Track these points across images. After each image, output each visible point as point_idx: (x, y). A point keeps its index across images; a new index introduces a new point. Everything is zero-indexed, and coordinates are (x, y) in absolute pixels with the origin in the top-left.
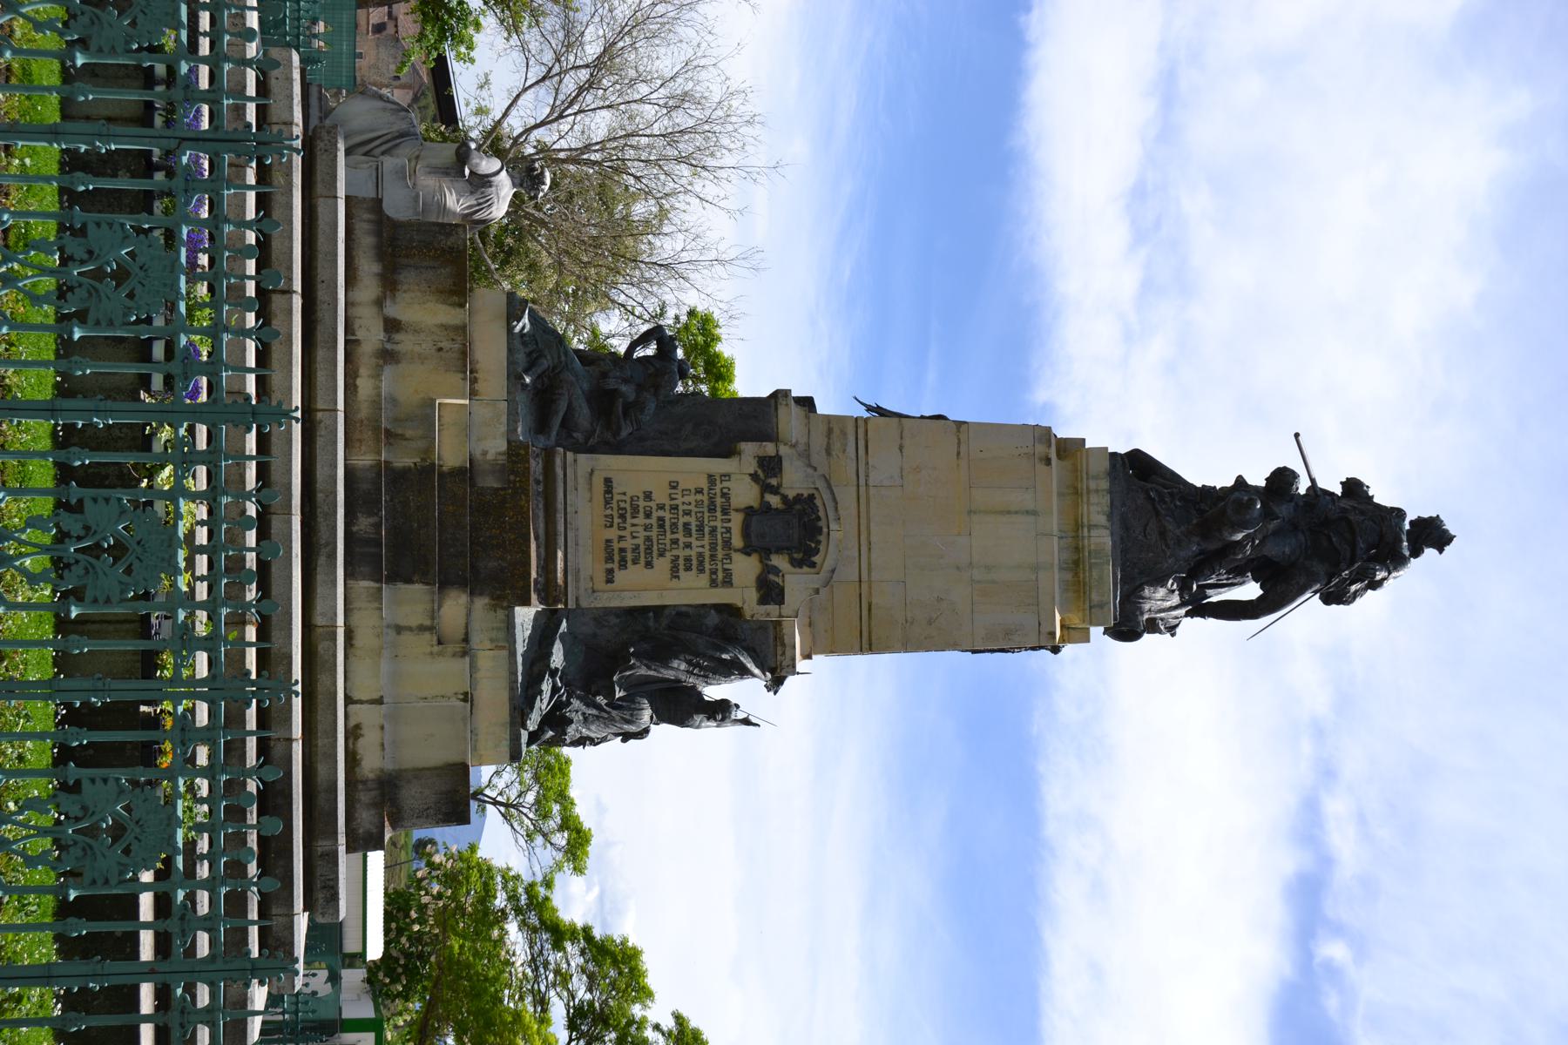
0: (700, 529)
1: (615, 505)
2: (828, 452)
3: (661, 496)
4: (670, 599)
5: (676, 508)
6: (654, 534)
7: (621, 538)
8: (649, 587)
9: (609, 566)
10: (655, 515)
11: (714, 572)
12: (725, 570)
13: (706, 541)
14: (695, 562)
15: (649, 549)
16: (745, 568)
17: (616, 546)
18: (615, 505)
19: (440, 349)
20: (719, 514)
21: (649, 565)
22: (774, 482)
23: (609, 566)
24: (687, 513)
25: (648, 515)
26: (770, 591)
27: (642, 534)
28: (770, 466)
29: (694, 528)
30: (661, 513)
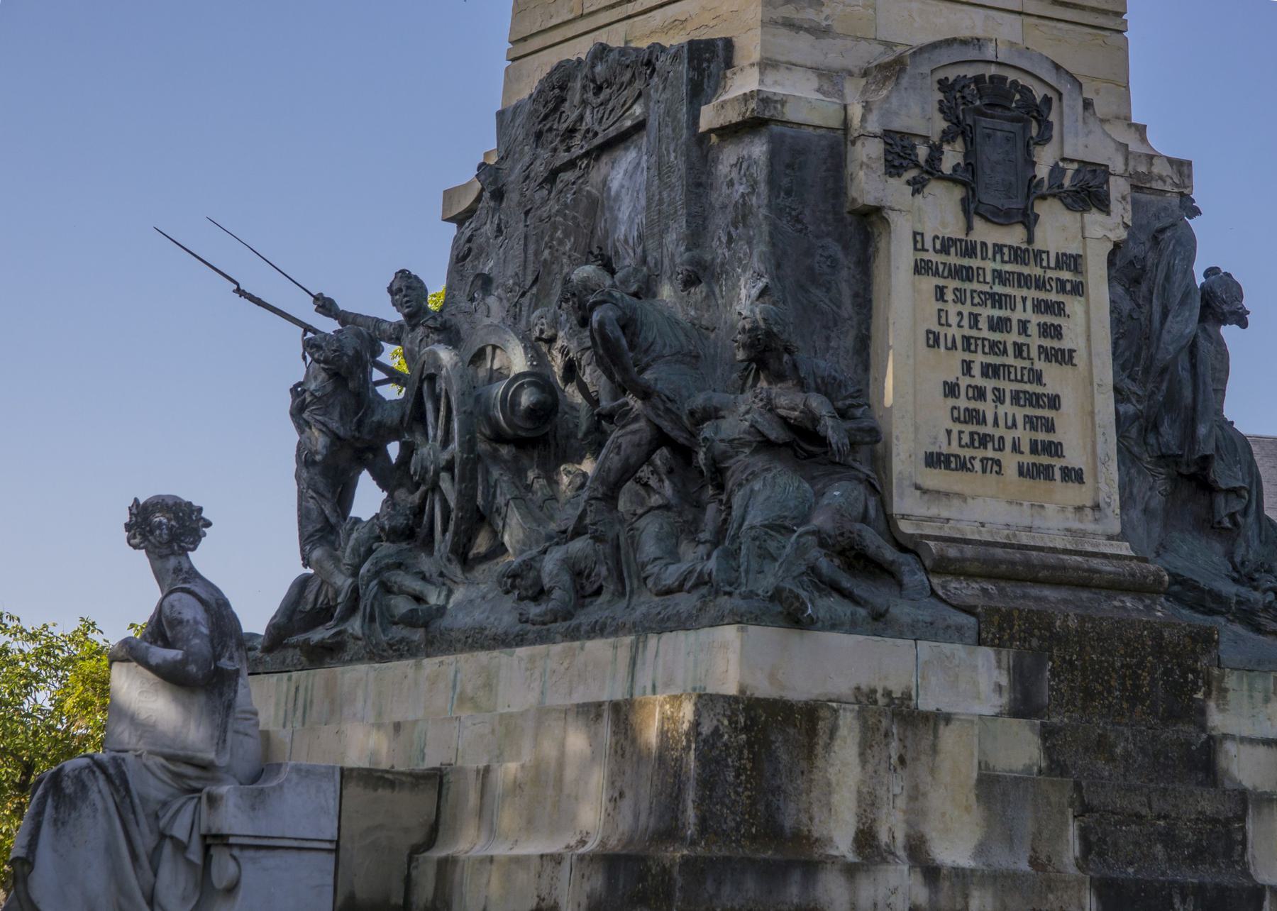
2: (819, 32)
3: (949, 366)
4: (1105, 372)
5: (966, 339)
6: (1008, 387)
7: (1016, 448)
10: (979, 381)
11: (1062, 285)
12: (1058, 266)
13: (1017, 292)
15: (1034, 400)
16: (1057, 229)
17: (1028, 459)
18: (967, 453)
19: (902, 760)
20: (975, 263)
21: (1054, 402)
22: (922, 152)
24: (975, 318)
25: (980, 394)
26: (1088, 192)
27: (1007, 408)
28: (899, 153)
29: (997, 313)
30: (976, 370)
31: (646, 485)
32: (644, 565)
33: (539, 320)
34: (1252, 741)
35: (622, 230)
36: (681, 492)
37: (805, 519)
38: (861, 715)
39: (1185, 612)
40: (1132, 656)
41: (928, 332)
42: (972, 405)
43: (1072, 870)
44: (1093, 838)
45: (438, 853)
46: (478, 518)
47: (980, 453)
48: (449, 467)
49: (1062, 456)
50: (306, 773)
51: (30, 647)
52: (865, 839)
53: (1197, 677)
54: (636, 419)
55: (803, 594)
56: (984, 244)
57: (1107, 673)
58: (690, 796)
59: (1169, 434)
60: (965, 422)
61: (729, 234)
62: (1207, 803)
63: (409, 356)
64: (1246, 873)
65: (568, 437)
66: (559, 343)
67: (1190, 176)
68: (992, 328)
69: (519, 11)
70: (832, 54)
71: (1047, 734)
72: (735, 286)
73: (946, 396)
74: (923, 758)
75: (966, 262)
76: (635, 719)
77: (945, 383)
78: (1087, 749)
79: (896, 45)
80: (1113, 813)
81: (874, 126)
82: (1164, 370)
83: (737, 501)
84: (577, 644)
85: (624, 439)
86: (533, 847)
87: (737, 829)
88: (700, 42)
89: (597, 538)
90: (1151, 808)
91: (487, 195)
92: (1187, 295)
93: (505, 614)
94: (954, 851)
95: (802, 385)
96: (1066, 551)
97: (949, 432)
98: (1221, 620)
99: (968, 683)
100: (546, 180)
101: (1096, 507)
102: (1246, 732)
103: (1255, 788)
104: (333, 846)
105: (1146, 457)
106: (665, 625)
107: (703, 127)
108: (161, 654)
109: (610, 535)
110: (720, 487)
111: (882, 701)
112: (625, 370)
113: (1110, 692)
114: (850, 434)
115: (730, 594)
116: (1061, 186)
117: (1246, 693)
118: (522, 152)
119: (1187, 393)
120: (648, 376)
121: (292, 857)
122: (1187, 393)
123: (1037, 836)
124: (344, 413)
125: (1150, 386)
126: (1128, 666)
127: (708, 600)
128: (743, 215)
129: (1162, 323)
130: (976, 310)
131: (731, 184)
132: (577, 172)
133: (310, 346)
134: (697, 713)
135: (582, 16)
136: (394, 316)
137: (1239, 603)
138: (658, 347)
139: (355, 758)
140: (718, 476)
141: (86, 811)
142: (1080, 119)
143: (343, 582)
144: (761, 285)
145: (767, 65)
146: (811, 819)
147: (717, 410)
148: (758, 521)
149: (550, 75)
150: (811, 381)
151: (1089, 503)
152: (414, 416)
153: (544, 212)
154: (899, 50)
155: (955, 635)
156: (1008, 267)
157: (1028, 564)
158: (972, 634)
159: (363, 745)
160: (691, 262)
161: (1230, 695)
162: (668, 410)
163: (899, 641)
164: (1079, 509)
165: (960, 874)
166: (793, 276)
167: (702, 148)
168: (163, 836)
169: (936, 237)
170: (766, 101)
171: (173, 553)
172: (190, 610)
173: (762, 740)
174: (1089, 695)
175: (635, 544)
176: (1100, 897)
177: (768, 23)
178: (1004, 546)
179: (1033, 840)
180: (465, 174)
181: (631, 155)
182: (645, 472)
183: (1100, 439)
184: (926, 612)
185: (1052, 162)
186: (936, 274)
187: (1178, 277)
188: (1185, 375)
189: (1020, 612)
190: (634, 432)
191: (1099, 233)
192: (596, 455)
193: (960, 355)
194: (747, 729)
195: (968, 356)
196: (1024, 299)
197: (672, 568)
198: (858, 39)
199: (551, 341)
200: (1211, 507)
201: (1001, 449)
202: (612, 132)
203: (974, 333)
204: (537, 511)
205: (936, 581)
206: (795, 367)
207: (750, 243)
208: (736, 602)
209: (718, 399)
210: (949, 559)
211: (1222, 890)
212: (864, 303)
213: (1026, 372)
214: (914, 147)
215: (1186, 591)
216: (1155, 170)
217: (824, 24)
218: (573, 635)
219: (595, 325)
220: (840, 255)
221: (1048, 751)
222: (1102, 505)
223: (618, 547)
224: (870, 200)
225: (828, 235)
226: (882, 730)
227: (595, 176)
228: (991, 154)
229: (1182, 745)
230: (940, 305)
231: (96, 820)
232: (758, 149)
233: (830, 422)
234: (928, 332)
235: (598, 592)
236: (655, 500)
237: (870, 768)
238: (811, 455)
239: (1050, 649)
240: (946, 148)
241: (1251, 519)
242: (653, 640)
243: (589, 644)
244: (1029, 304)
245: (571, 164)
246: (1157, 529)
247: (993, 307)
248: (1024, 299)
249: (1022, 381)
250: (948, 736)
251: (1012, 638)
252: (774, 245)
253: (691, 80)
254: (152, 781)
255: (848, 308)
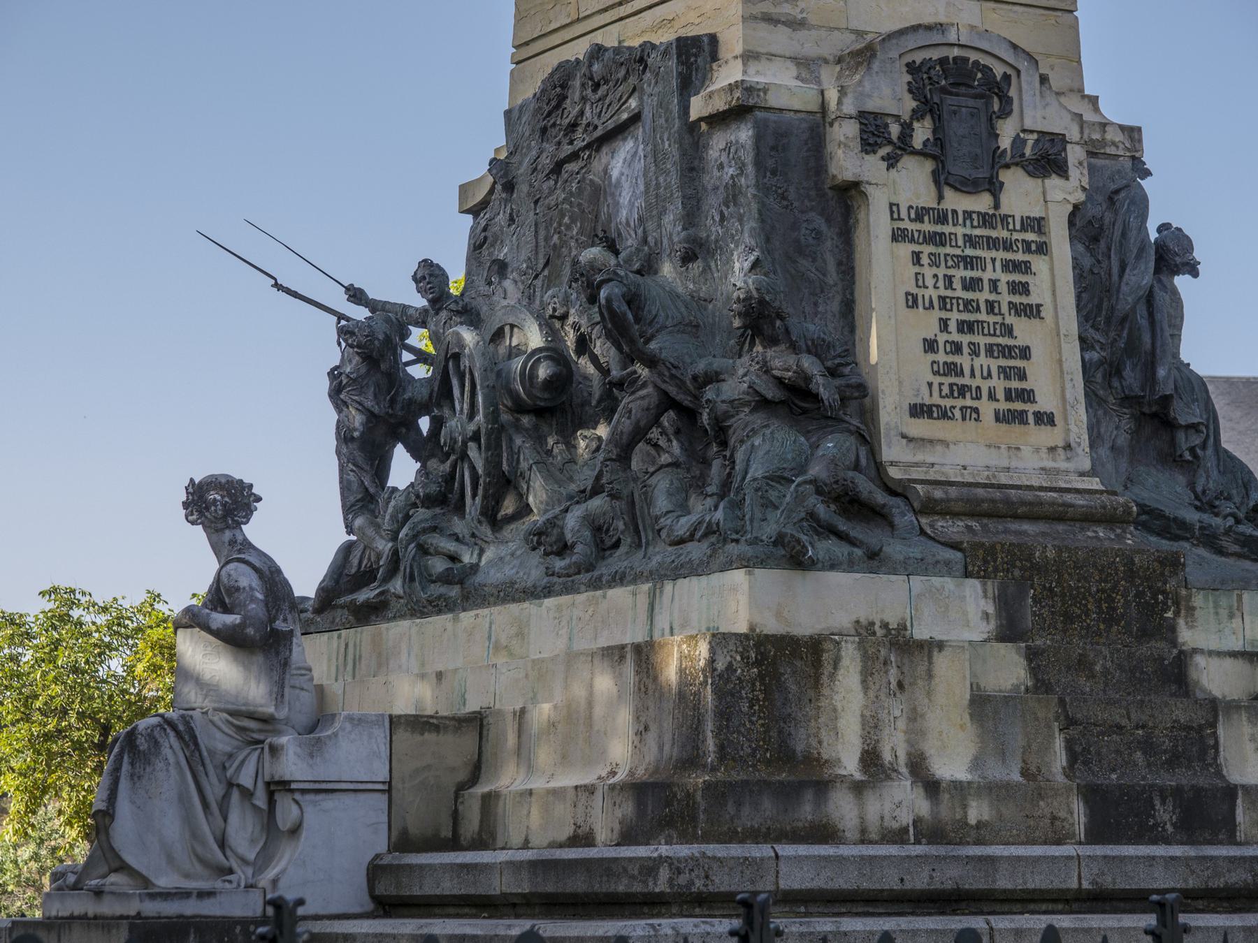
0: (969, 262)
1: (948, 403)
2: (797, 24)
3: (927, 323)
4: (1070, 323)
5: (942, 299)
6: (983, 341)
7: (992, 397)
8: (1055, 359)
9: (1031, 419)
10: (955, 337)
11: (1027, 246)
12: (1024, 229)
13: (986, 254)
14: (1017, 277)
15: (1007, 352)
16: (1020, 194)
17: (1003, 406)
18: (948, 403)
19: (900, 685)
20: (947, 229)
21: (1025, 353)
22: (895, 130)
23: (1031, 419)
24: (949, 280)
25: (957, 348)
26: (1047, 159)
27: (982, 360)
28: (873, 132)
29: (969, 274)
30: (953, 326)
31: (656, 446)
32: (657, 518)
33: (551, 299)
34: (1220, 654)
35: (624, 213)
36: (688, 450)
37: (802, 469)
38: (861, 645)
39: (1153, 539)
40: (1106, 581)
41: (907, 294)
42: (950, 359)
43: (1060, 778)
44: (1078, 749)
45: (481, 789)
46: (504, 482)
47: (960, 403)
48: (476, 437)
49: (1034, 402)
50: (358, 722)
51: (102, 619)
52: (870, 759)
53: (1166, 598)
54: (644, 385)
55: (804, 538)
56: (954, 212)
57: (1084, 598)
58: (709, 726)
59: (1131, 377)
60: (944, 375)
61: (722, 214)
62: (1180, 712)
63: (435, 338)
64: (1219, 774)
65: (582, 405)
66: (571, 320)
67: (1140, 141)
68: (965, 288)
69: (521, 18)
70: (807, 43)
71: (1032, 656)
72: (729, 261)
73: (926, 352)
74: (920, 683)
75: (939, 228)
76: (658, 658)
77: (925, 340)
78: (1069, 668)
79: (867, 33)
80: (1095, 725)
81: (849, 108)
82: (1124, 319)
83: (740, 456)
84: (599, 593)
85: (633, 404)
86: (568, 780)
87: (753, 755)
88: (687, 38)
89: (614, 496)
90: (1129, 719)
91: (499, 187)
92: (1142, 249)
93: (533, 569)
94: (952, 765)
95: (794, 348)
96: (1041, 489)
97: (930, 385)
98: (1186, 545)
99: (958, 612)
100: (552, 172)
101: (1068, 447)
102: (1214, 646)
103: (1224, 697)
104: (386, 787)
105: (1111, 399)
106: (678, 572)
107: (694, 116)
108: (221, 619)
109: (625, 492)
110: (724, 444)
111: (880, 632)
112: (632, 342)
113: (1087, 615)
114: (839, 389)
115: (737, 541)
116: (1023, 155)
117: (1212, 611)
118: (529, 147)
119: (1147, 338)
120: (653, 345)
121: (348, 799)
122: (1147, 338)
123: (1026, 749)
124: (379, 391)
125: (1112, 334)
126: (1103, 591)
127: (718, 546)
128: (733, 195)
129: (1121, 276)
130: (950, 272)
131: (721, 167)
132: (580, 163)
133: (346, 332)
134: (712, 650)
135: (578, 20)
136: (419, 302)
137: (1201, 528)
138: (661, 319)
139: (402, 707)
140: (721, 433)
141: (160, 765)
142: (1038, 93)
143: (384, 546)
144: (752, 258)
145: (749, 56)
146: (820, 742)
147: (717, 373)
148: (759, 474)
149: (551, 75)
150: (802, 343)
151: (1061, 444)
152: (441, 392)
153: (551, 200)
154: (869, 37)
155: (945, 568)
156: (977, 232)
157: (1007, 502)
158: (960, 567)
159: (410, 694)
160: (688, 240)
161: (1197, 613)
162: (673, 377)
163: (893, 577)
164: (1051, 448)
165: (957, 786)
166: (783, 249)
167: (693, 136)
168: (230, 785)
169: (910, 207)
170: (749, 89)
171: (228, 527)
172: (246, 579)
173: (773, 672)
174: (1068, 618)
175: (649, 500)
176: (1086, 802)
177: (748, 19)
178: (985, 486)
179: (1024, 753)
180: (477, 169)
181: (630, 144)
182: (654, 433)
183: (1068, 385)
184: (917, 549)
185: (1013, 134)
186: (912, 240)
187: (1133, 234)
188: (1144, 323)
189: (1003, 545)
190: (643, 398)
191: (1059, 196)
192: (609, 420)
193: (937, 314)
194: (758, 663)
195: (944, 315)
196: (993, 260)
197: (683, 520)
198: (831, 29)
199: (563, 318)
200: (1173, 443)
201: (978, 398)
202: (611, 125)
203: (949, 293)
204: (558, 473)
205: (924, 521)
206: (787, 331)
207: (741, 220)
208: (743, 548)
209: (718, 363)
210: (935, 500)
211: (1198, 791)
212: (848, 270)
213: (998, 327)
214: (887, 125)
215: (1153, 520)
216: (1109, 137)
217: (800, 17)
218: (596, 585)
219: (603, 301)
220: (824, 228)
221: (1034, 671)
222: (1073, 445)
223: (633, 503)
224: (849, 176)
225: (812, 209)
226: (882, 659)
227: (597, 165)
228: (957, 128)
229: (1155, 660)
230: (917, 269)
231: (169, 772)
232: (744, 134)
233: (820, 380)
234: (907, 294)
235: (617, 545)
236: (665, 458)
237: (871, 694)
238: (805, 412)
239: (1031, 578)
240: (916, 125)
241: (1210, 451)
242: (668, 586)
243: (611, 593)
244: (998, 264)
245: (574, 156)
246: (1124, 464)
247: (966, 268)
248: (993, 260)
249: (995, 335)
250: (942, 662)
251: (996, 570)
252: (763, 221)
253: (680, 74)
254: (219, 735)
255: (833, 276)
